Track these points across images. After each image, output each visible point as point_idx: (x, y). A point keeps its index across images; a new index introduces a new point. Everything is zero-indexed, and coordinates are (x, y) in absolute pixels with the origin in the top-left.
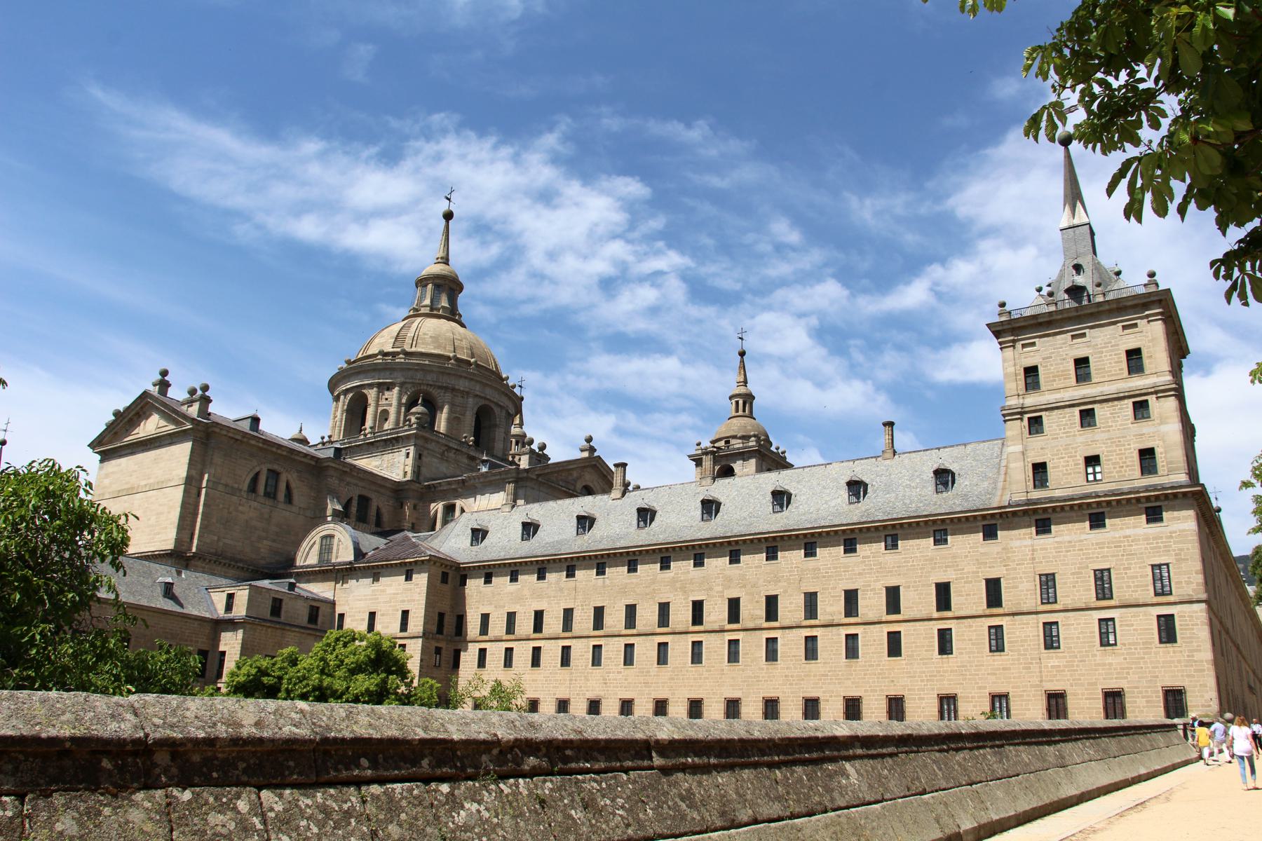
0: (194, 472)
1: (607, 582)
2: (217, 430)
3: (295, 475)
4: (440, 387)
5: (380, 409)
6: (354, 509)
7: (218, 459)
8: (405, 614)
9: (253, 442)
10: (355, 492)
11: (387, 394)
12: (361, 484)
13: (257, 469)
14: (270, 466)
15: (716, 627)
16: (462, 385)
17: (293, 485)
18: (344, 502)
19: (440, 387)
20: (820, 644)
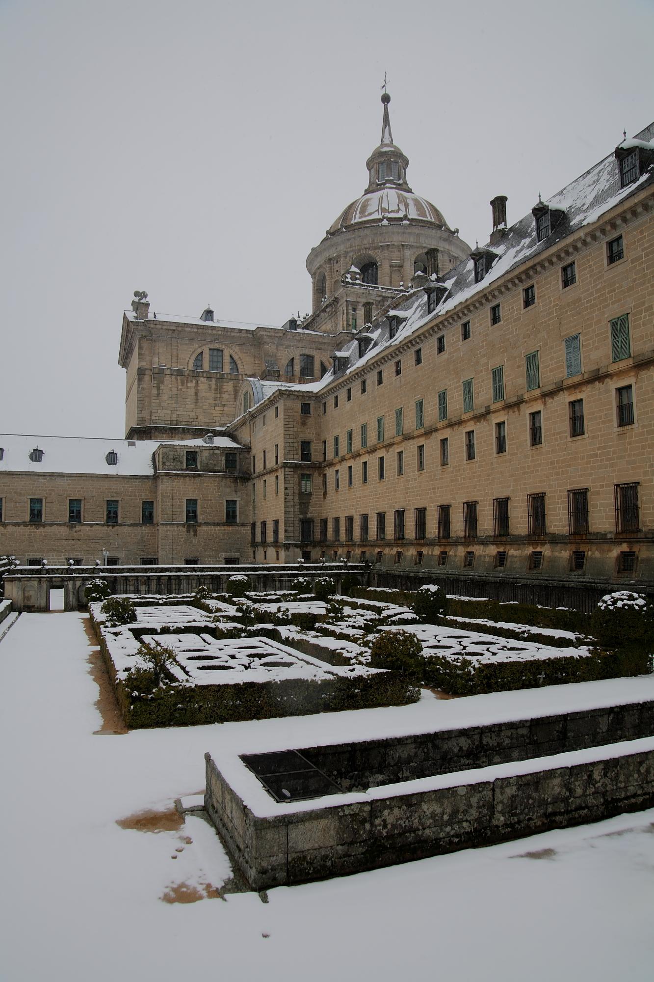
0: (144, 364)
1: (403, 380)
2: (152, 326)
3: (237, 349)
4: (377, 248)
5: (333, 280)
6: (297, 368)
7: (161, 348)
8: (277, 446)
9: (188, 329)
10: (296, 354)
11: (336, 267)
12: (300, 345)
13: (199, 351)
14: (212, 346)
15: (483, 410)
16: (397, 239)
17: (236, 357)
18: (285, 362)
19: (377, 248)
20: (587, 410)
